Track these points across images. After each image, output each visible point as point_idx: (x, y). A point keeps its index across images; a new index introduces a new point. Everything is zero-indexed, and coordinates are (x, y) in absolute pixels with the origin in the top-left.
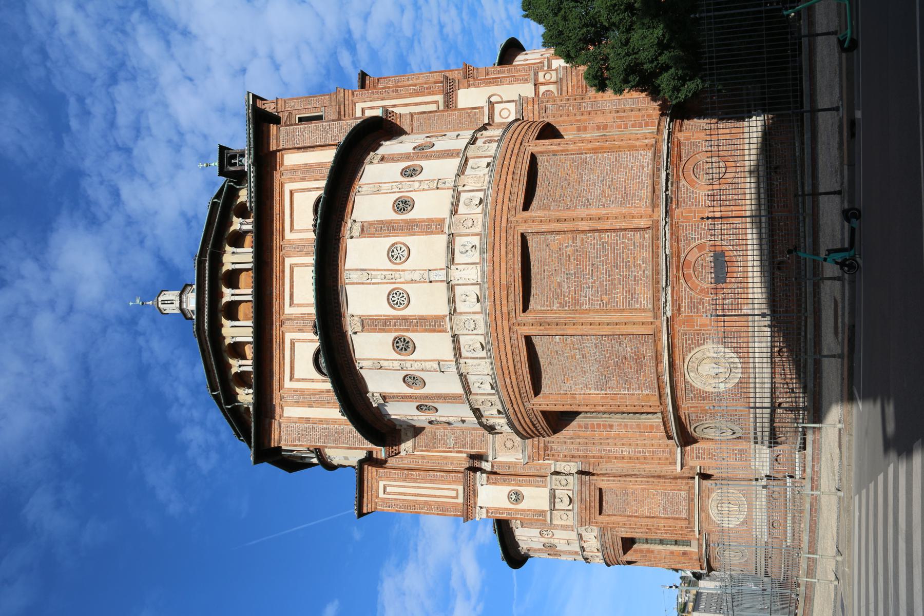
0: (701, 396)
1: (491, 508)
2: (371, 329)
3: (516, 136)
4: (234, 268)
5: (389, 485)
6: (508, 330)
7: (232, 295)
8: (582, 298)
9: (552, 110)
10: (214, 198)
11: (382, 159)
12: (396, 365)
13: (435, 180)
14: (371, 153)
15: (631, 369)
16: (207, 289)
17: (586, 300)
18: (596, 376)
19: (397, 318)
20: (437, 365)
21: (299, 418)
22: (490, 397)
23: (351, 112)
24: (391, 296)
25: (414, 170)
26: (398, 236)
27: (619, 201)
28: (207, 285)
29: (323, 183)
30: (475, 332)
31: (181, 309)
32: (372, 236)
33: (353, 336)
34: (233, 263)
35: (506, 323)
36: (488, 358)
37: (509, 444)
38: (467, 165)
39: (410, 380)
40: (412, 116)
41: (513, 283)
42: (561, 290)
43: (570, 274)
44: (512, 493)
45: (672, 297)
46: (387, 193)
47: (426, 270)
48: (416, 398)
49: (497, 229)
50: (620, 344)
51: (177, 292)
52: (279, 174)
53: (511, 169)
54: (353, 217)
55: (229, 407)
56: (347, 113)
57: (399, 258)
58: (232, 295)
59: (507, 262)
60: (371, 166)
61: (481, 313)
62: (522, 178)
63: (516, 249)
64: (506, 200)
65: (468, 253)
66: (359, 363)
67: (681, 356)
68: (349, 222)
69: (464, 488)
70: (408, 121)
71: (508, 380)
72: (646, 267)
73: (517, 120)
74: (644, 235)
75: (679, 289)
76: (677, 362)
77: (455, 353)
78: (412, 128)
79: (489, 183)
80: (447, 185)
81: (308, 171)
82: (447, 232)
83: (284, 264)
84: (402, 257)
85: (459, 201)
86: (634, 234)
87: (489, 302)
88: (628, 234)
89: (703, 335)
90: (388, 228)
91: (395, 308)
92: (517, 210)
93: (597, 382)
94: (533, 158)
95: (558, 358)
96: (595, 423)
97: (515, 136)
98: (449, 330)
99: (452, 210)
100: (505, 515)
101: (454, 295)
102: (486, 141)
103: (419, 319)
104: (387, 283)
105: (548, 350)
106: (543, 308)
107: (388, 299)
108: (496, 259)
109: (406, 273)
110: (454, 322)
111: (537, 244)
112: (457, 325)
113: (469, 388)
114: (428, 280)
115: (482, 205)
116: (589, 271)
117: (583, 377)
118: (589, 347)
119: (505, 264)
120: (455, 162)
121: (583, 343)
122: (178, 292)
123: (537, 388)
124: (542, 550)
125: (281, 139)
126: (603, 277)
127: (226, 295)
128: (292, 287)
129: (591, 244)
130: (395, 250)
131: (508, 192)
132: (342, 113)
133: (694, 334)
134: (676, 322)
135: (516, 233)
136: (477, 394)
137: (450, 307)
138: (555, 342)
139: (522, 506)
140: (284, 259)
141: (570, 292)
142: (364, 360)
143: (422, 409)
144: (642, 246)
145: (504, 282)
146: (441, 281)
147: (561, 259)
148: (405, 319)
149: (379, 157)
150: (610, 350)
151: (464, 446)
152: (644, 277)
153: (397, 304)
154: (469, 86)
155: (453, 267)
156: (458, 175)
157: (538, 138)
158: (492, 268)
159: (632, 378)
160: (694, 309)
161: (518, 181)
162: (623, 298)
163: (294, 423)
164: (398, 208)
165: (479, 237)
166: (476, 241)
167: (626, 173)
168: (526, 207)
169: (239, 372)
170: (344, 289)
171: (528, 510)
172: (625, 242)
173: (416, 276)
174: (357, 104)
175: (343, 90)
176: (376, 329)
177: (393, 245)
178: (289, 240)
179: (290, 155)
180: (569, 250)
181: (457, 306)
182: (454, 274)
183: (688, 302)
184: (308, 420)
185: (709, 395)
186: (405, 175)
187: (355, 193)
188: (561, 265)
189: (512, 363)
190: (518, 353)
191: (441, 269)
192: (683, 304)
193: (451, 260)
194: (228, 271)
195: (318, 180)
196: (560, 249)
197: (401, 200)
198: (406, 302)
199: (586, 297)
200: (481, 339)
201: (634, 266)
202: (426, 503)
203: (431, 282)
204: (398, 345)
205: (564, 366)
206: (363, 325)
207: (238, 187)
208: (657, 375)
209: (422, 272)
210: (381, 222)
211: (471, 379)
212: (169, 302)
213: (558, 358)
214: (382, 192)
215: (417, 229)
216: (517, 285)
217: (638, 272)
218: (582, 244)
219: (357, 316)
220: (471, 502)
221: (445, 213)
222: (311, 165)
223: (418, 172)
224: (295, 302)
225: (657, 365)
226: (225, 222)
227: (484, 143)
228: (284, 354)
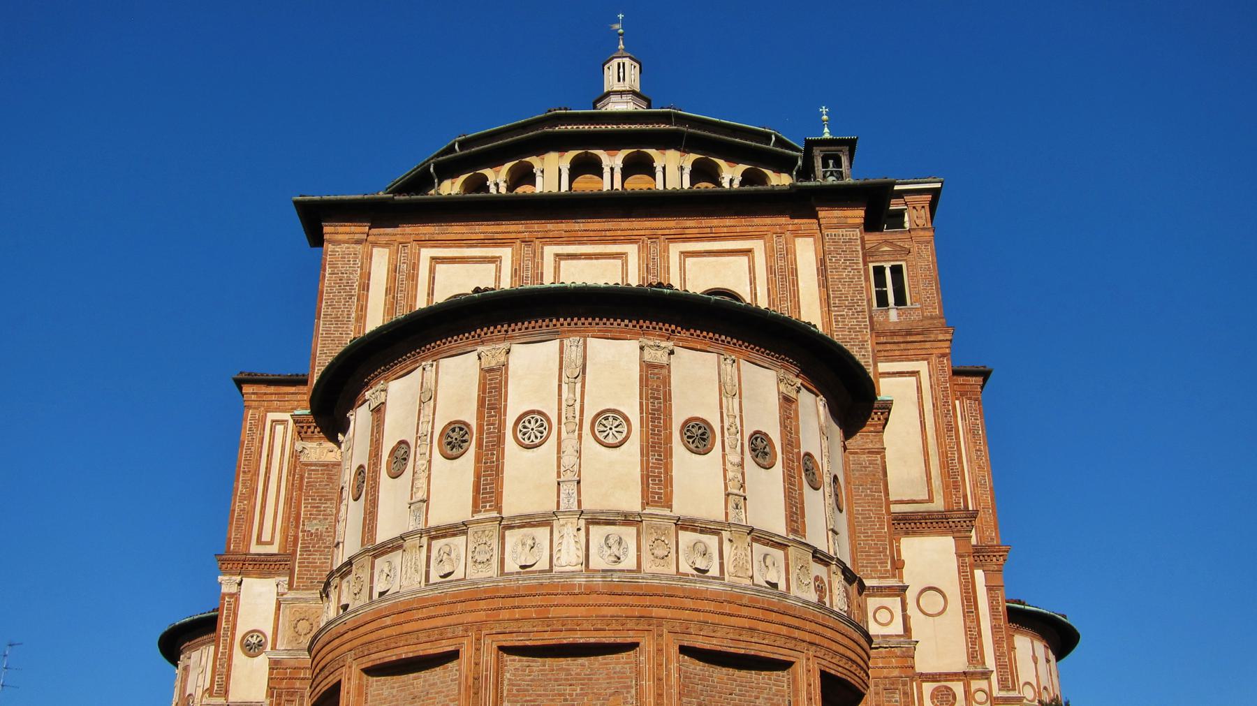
1: (237, 600)
2: (485, 384)
3: (829, 635)
4: (657, 170)
5: (286, 429)
6: (470, 620)
7: (612, 169)
9: (890, 701)
11: (787, 400)
12: (425, 428)
13: (744, 491)
16: (621, 127)
19: (501, 426)
20: (419, 499)
21: (369, 273)
22: (366, 591)
23: (911, 352)
24: (538, 417)
25: (766, 454)
26: (642, 426)
28: (627, 127)
29: (763, 303)
31: (609, 94)
32: (644, 382)
33: (474, 355)
34: (664, 168)
35: (482, 616)
36: (426, 585)
37: (303, 626)
38: (772, 546)
39: (401, 454)
40: (878, 453)
41: (549, 629)
44: (261, 637)
46: (721, 407)
47: (579, 475)
48: (374, 464)
49: (647, 601)
51: (639, 87)
52: (779, 231)
53: (761, 626)
54: (677, 349)
55: (432, 170)
56: (909, 346)
57: (602, 428)
58: (612, 169)
59: (587, 618)
60: (774, 381)
61: (502, 573)
62: (743, 645)
64: (701, 616)
65: (605, 548)
66: (432, 365)
68: (670, 344)
69: (272, 555)
70: (871, 446)
71: (388, 621)
73: (869, 639)
77: (437, 529)
78: (856, 453)
79: (732, 586)
80: (731, 512)
81: (783, 277)
82: (644, 512)
84: (605, 434)
85: (702, 532)
90: (657, 410)
91: (517, 423)
92: (680, 636)
94: (785, 665)
97: (829, 633)
98: (477, 517)
99: (685, 520)
100: (224, 625)
101: (534, 526)
102: (822, 581)
103: (498, 466)
105: (437, 693)
106: (506, 682)
107: (533, 412)
108: (592, 599)
109: (575, 442)
110: (489, 526)
111: (619, 672)
112: (484, 531)
114: (562, 478)
115: (695, 572)
119: (584, 614)
120: (777, 525)
122: (638, 89)
123: (376, 671)
124: (184, 692)
125: (840, 231)
127: (612, 158)
128: (588, 256)
130: (617, 423)
131: (717, 619)
132: (909, 339)
135: (640, 634)
136: (373, 568)
137: (514, 517)
139: (239, 656)
140: (636, 243)
142: (437, 373)
143: (360, 474)
145: (553, 612)
146: (558, 503)
148: (500, 440)
149: (793, 395)
151: (305, 549)
153: (525, 427)
154: (959, 556)
155: (582, 523)
156: (751, 532)
157: (825, 676)
158: (577, 591)
161: (737, 637)
163: (362, 264)
164: (693, 427)
165: (635, 568)
166: (629, 562)
168: (684, 650)
169: (488, 183)
170: (553, 337)
171: (230, 666)
173: (569, 459)
174: (926, 362)
175: (949, 338)
176: (484, 392)
177: (627, 419)
178: (667, 250)
179: (812, 248)
181: (516, 530)
182: (569, 525)
184: (365, 287)
186: (756, 439)
187: (723, 352)
191: (579, 502)
193: (595, 520)
194: (653, 161)
195: (769, 296)
197: (708, 431)
198: (527, 442)
200: (459, 574)
202: (254, 491)
203: (559, 484)
204: (457, 430)
206: (491, 370)
207: (795, 173)
209: (576, 468)
210: (668, 397)
211: (396, 557)
212: (621, 75)
214: (724, 399)
215: (652, 460)
219: (508, 361)
220: (250, 568)
221: (682, 506)
222: (795, 283)
223: (760, 460)
224: (563, 263)
226: (735, 155)
227: (817, 578)
228: (476, 247)
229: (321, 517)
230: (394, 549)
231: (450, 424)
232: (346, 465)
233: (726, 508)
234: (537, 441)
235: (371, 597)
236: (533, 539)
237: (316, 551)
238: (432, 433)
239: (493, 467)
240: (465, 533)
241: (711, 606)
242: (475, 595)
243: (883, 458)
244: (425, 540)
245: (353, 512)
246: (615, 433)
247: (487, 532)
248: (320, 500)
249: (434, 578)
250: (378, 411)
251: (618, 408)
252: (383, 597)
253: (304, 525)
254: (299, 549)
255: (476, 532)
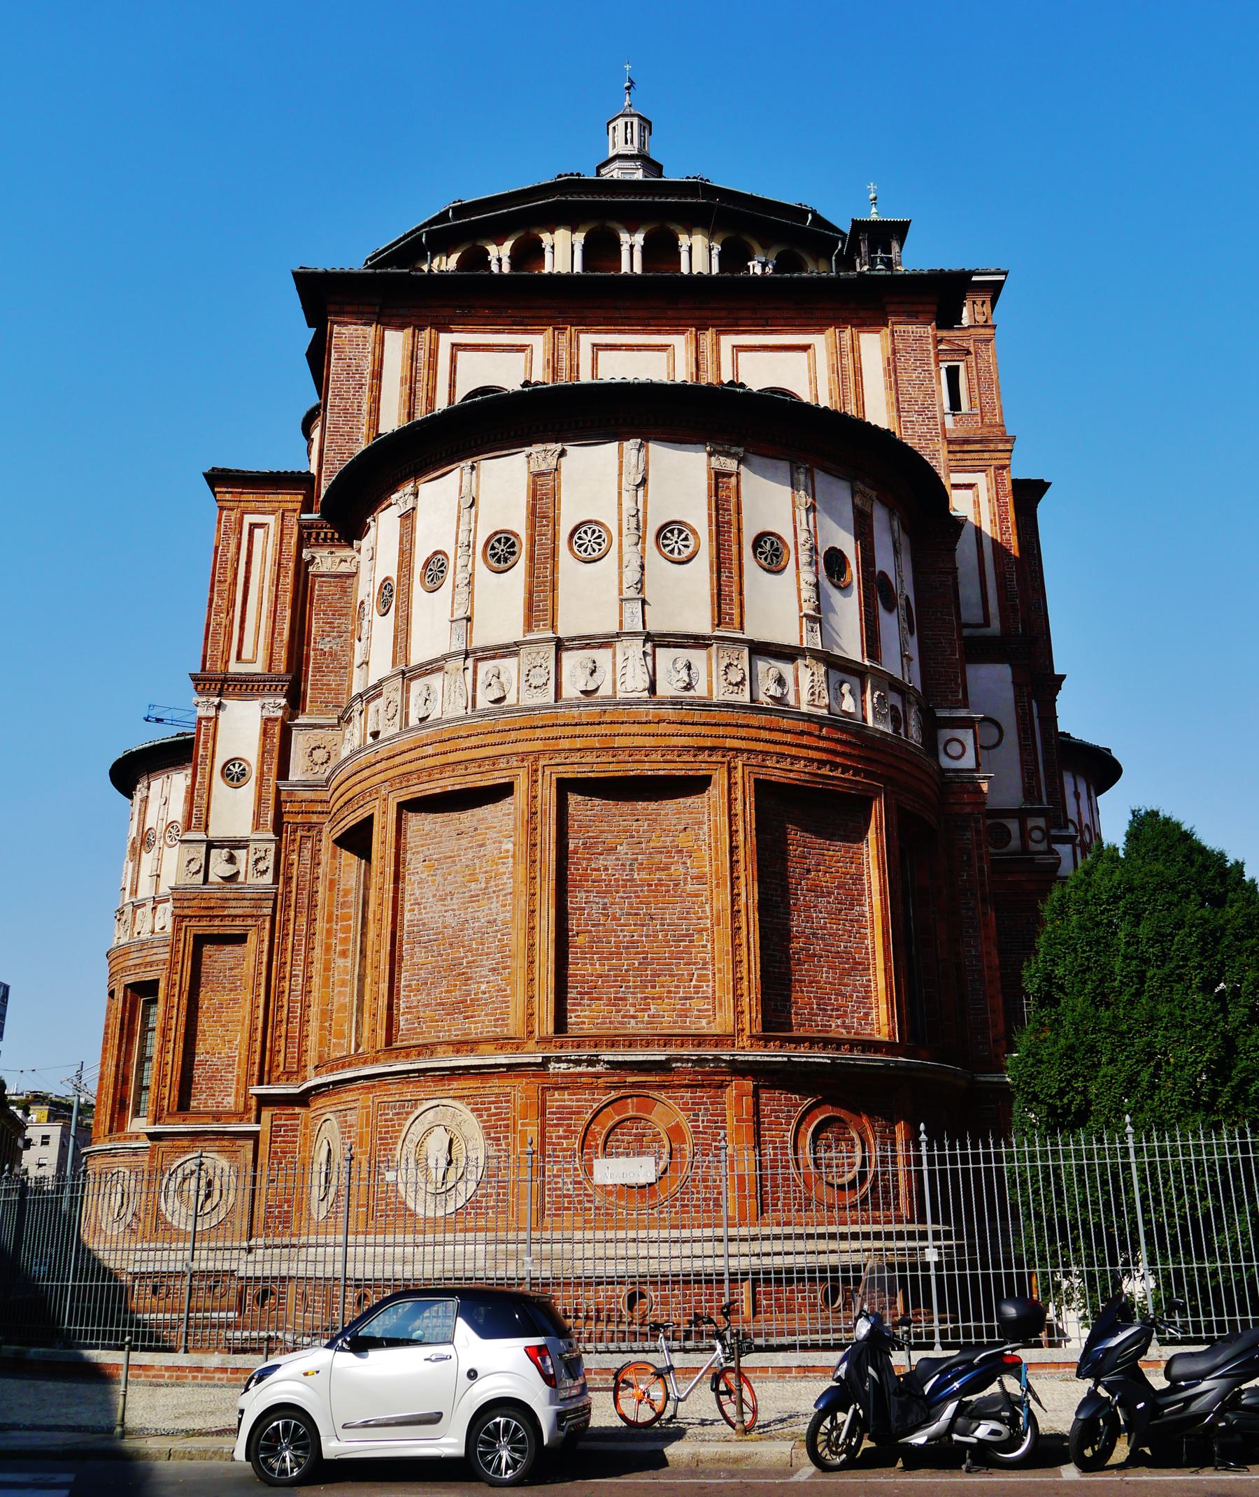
0: (387, 1132)
8: (584, 895)
10: (814, 213)
14: (875, 493)
15: (447, 992)
17: (581, 902)
18: (436, 922)
27: (775, 967)
29: (824, 402)
30: (524, 686)
35: (538, 745)
37: (320, 755)
39: (436, 568)
41: (614, 759)
42: (601, 854)
43: (632, 870)
45: (581, 1075)
49: (721, 731)
50: (494, 969)
59: (655, 748)
63: (680, 766)
64: (778, 748)
65: (674, 673)
67: (466, 1093)
71: (430, 750)
72: (642, 1022)
74: (705, 1017)
75: (597, 1088)
76: (455, 1084)
77: (484, 649)
83: (673, 334)
84: (670, 548)
86: (707, 998)
87: (580, 715)
88: (707, 986)
89: (506, 1138)
92: (756, 770)
93: (424, 924)
95: (472, 847)
96: (351, 922)
98: (530, 637)
101: (593, 648)
104: (620, 520)
107: (590, 522)
108: (662, 729)
113: (420, 676)
116: (638, 909)
117: (434, 896)
118: (490, 909)
119: (653, 744)
121: (498, 897)
126: (625, 936)
129: (688, 913)
130: (683, 536)
131: (794, 751)
132: (967, 447)
133: (508, 1119)
134: (532, 1082)
138: (500, 842)
141: (598, 870)
144: (684, 1014)
145: (619, 742)
146: (621, 622)
147: (661, 852)
150: (483, 950)
152: (623, 1017)
153: (580, 538)
158: (644, 719)
159: (429, 994)
160: (558, 1119)
162: (583, 976)
167: (830, 983)
172: (691, 981)
177: (694, 532)
180: (677, 870)
182: (634, 647)
183: (571, 1107)
185: (391, 1150)
188: (650, 853)
189: (463, 759)
190: (482, 769)
192: (566, 1097)
196: (681, 851)
198: (584, 555)
199: (586, 903)
201: (646, 998)
205: (457, 859)
208: (433, 1044)
211: (436, 680)
213: (472, 847)
216: (611, 767)
217: (634, 1005)
218: (689, 895)
221: (754, 631)
225: (449, 1043)
229: (335, 634)
230: (433, 672)
231: (496, 533)
232: (364, 575)
233: (801, 631)
234: (595, 555)
235: (407, 724)
236: (594, 662)
237: (331, 672)
238: (474, 542)
239: (547, 582)
240: (516, 654)
241: (788, 738)
242: (530, 720)
243: (955, 578)
244: (470, 662)
245: (381, 629)
246: (681, 547)
247: (542, 654)
248: (334, 615)
249: (483, 702)
250: (408, 517)
251: (684, 520)
252: (424, 724)
253: (315, 643)
254: (310, 669)
255: (530, 654)
